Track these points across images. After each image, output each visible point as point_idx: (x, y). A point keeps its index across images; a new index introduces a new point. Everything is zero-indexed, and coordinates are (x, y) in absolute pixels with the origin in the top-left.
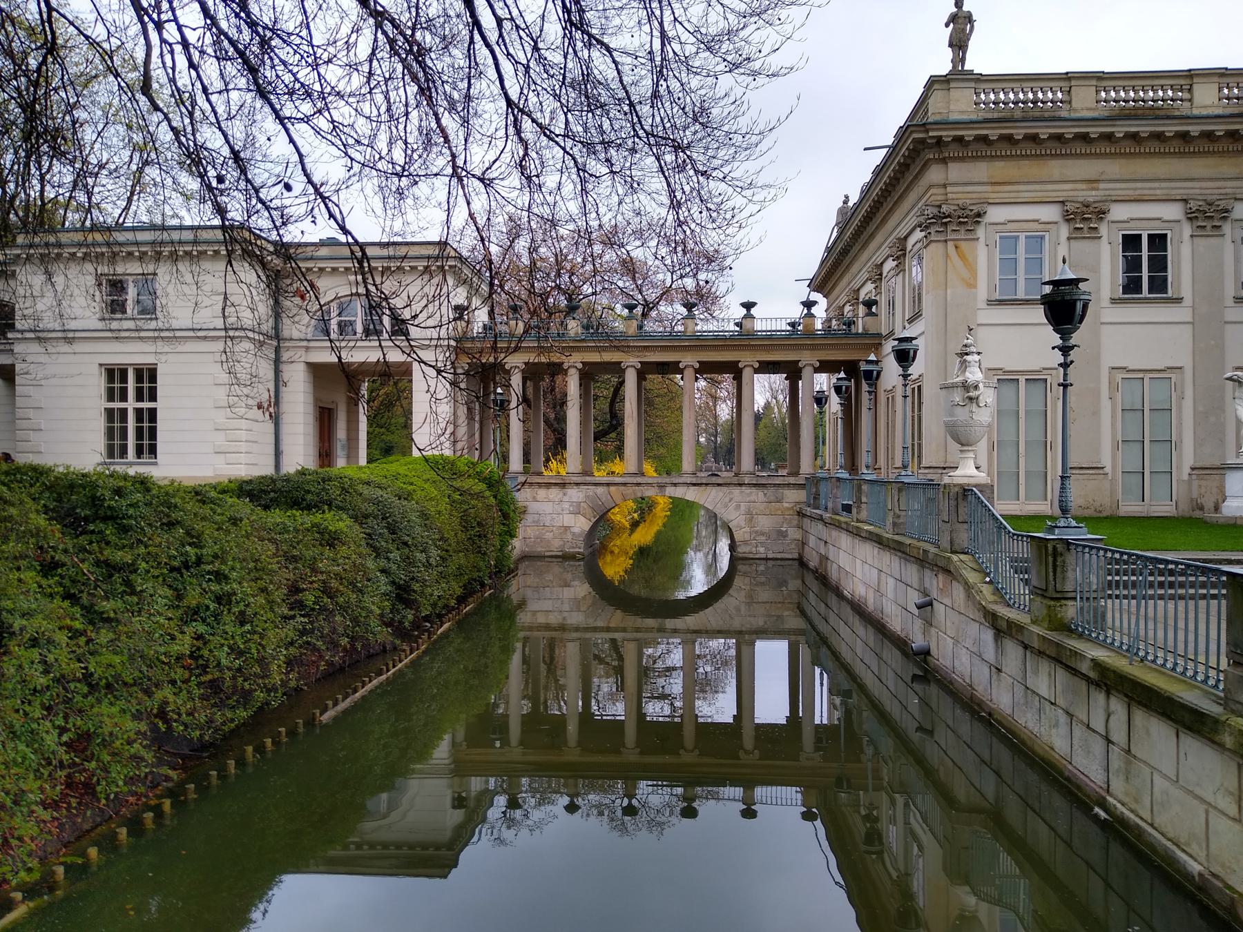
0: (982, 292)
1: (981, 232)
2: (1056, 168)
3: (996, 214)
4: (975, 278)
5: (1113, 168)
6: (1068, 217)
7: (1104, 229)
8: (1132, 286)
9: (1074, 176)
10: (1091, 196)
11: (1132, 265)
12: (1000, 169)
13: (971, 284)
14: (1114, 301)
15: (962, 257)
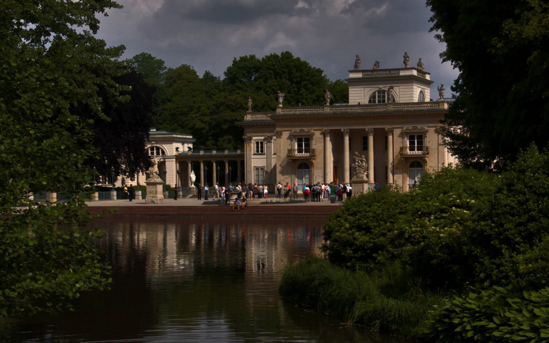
13: (251, 151)
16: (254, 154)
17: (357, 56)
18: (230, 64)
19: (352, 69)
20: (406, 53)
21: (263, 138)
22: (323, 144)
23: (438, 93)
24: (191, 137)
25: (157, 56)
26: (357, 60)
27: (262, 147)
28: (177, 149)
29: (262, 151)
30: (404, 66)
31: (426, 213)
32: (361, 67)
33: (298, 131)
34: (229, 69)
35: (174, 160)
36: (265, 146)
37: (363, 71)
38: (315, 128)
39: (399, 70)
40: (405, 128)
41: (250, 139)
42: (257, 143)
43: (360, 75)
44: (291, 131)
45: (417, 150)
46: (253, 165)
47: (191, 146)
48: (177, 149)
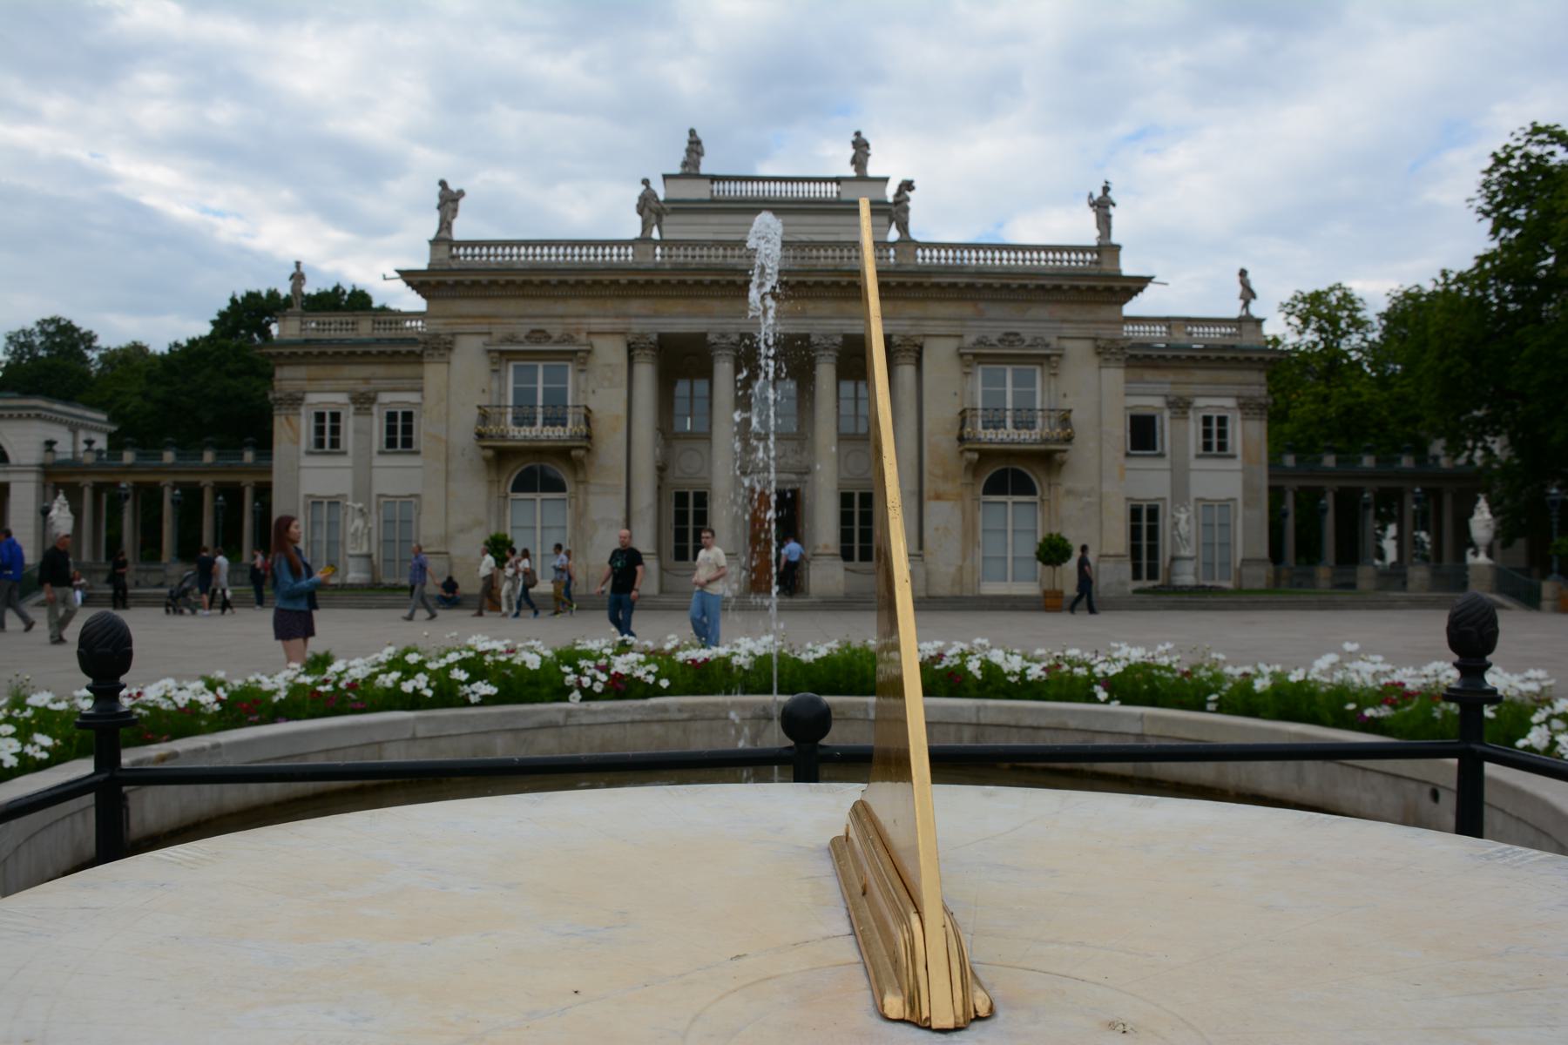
0: (303, 446)
1: (303, 410)
2: (348, 371)
3: (312, 398)
4: (298, 436)
5: (380, 370)
6: (354, 400)
7: (375, 409)
8: (391, 443)
9: (356, 375)
10: (362, 387)
11: (391, 430)
12: (315, 371)
13: (297, 442)
14: (381, 453)
15: (290, 425)
16: (309, 453)
17: (692, 132)
18: (225, 305)
19: (677, 170)
20: (858, 134)
21: (342, 398)
22: (623, 392)
23: (1091, 217)
24: (104, 417)
25: (83, 323)
26: (691, 143)
27: (335, 430)
28: (50, 444)
29: (335, 443)
30: (850, 172)
31: (1091, 680)
32: (705, 169)
33: (522, 337)
34: (222, 314)
35: (33, 477)
36: (349, 424)
37: (714, 179)
38: (594, 328)
39: (838, 180)
40: (970, 339)
41: (295, 401)
42: (320, 417)
43: (699, 191)
44: (490, 334)
45: (1016, 427)
46: (304, 491)
47: (101, 443)
48: (50, 444)
